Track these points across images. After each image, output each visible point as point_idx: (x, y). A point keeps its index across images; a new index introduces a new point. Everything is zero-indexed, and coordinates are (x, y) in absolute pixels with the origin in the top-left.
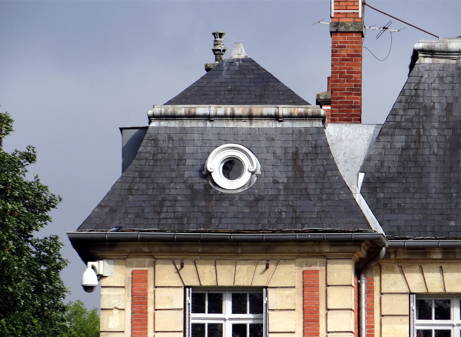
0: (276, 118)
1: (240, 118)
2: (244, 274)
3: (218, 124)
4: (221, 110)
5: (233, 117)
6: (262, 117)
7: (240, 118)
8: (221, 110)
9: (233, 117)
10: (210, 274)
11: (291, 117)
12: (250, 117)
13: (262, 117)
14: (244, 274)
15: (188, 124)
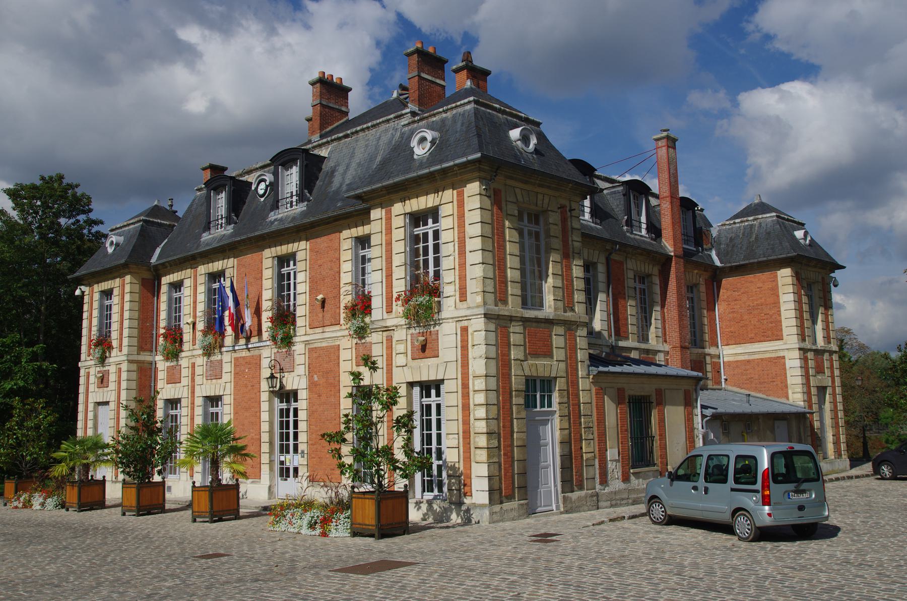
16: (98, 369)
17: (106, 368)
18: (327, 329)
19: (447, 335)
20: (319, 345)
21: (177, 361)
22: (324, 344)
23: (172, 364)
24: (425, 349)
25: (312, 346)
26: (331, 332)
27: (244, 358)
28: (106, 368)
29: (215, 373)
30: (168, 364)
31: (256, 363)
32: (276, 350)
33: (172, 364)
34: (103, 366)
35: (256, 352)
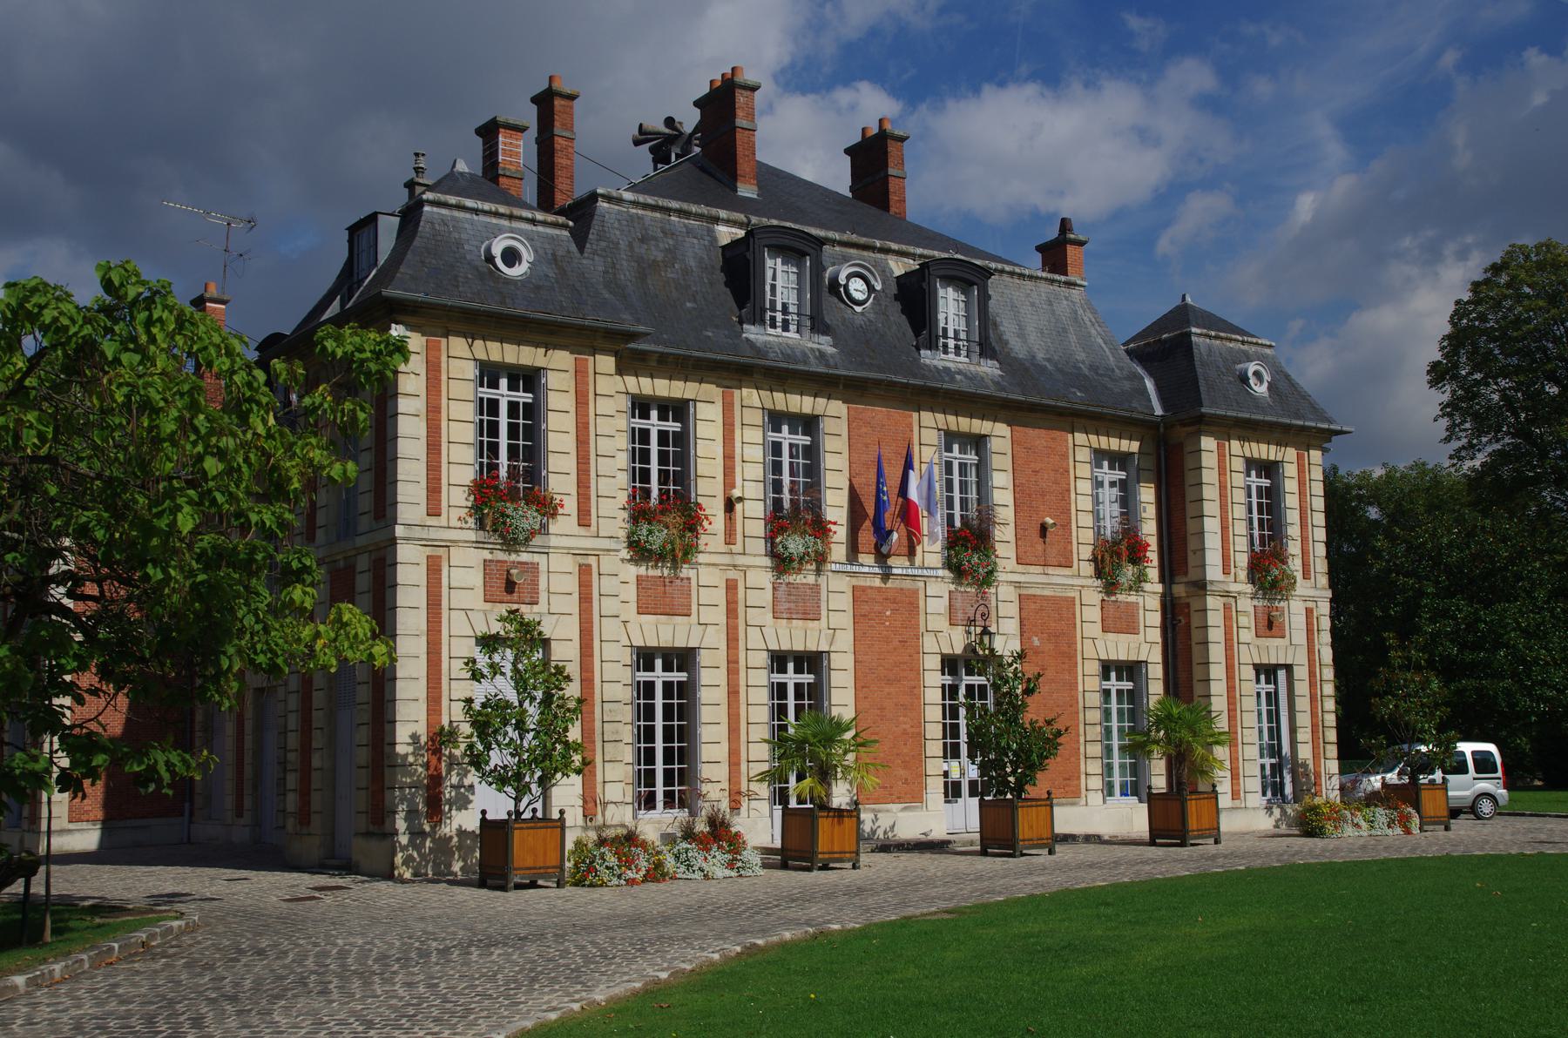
0: (533, 221)
1: (501, 216)
2: (527, 356)
3: (482, 218)
4: (487, 206)
5: (496, 214)
6: (521, 219)
7: (501, 216)
8: (487, 206)
9: (496, 214)
10: (497, 352)
11: (544, 223)
12: (511, 217)
13: (521, 219)
14: (527, 356)
15: (457, 214)
16: (487, 555)
17: (524, 557)
18: (1050, 570)
19: (1294, 611)
20: (1038, 592)
21: (675, 567)
22: (1047, 593)
23: (651, 572)
24: (1270, 625)
25: (1024, 592)
26: (1058, 576)
27: (879, 589)
28: (524, 557)
29: (806, 607)
30: (632, 572)
31: (909, 605)
32: (952, 587)
33: (651, 572)
34: (509, 551)
35: (907, 584)
